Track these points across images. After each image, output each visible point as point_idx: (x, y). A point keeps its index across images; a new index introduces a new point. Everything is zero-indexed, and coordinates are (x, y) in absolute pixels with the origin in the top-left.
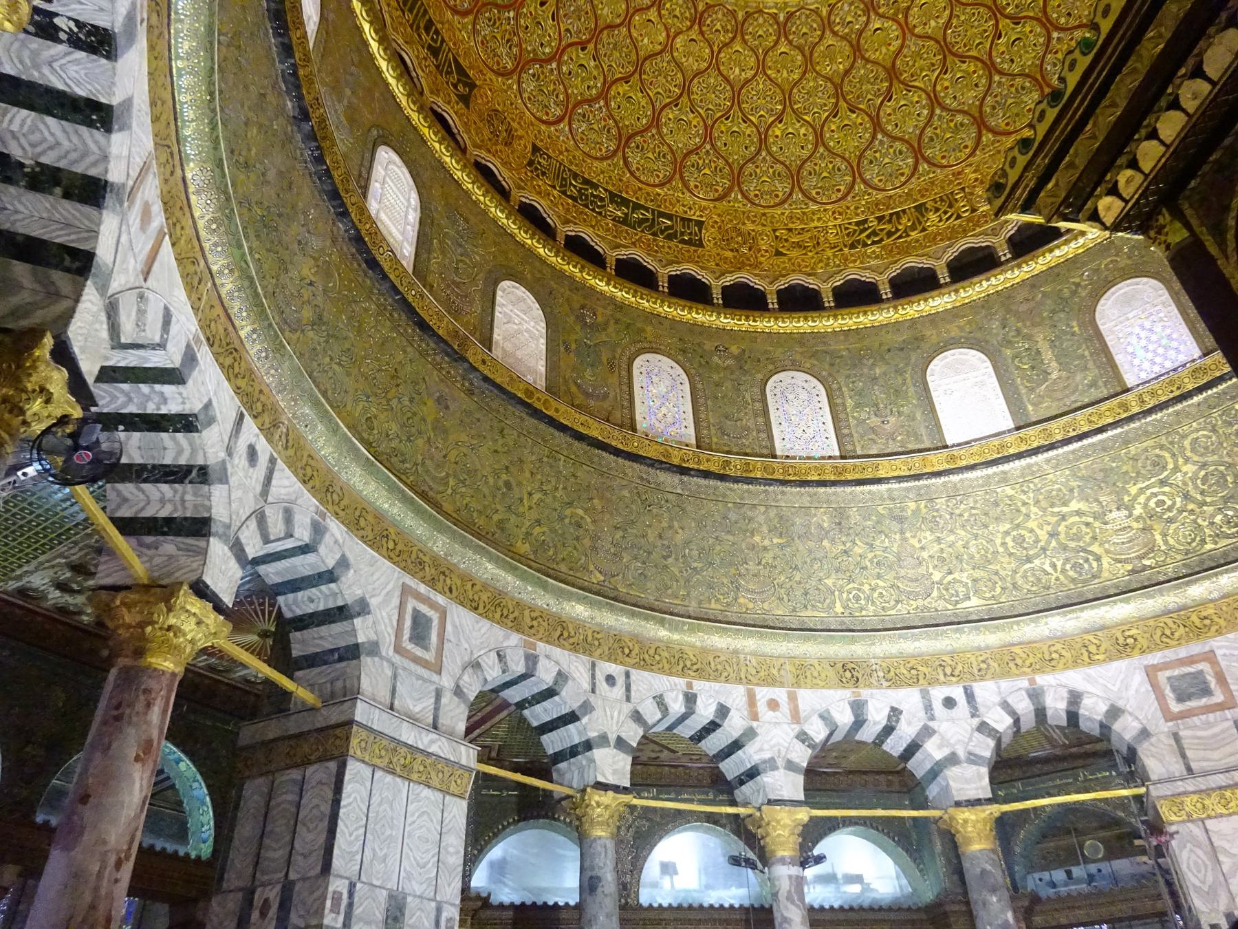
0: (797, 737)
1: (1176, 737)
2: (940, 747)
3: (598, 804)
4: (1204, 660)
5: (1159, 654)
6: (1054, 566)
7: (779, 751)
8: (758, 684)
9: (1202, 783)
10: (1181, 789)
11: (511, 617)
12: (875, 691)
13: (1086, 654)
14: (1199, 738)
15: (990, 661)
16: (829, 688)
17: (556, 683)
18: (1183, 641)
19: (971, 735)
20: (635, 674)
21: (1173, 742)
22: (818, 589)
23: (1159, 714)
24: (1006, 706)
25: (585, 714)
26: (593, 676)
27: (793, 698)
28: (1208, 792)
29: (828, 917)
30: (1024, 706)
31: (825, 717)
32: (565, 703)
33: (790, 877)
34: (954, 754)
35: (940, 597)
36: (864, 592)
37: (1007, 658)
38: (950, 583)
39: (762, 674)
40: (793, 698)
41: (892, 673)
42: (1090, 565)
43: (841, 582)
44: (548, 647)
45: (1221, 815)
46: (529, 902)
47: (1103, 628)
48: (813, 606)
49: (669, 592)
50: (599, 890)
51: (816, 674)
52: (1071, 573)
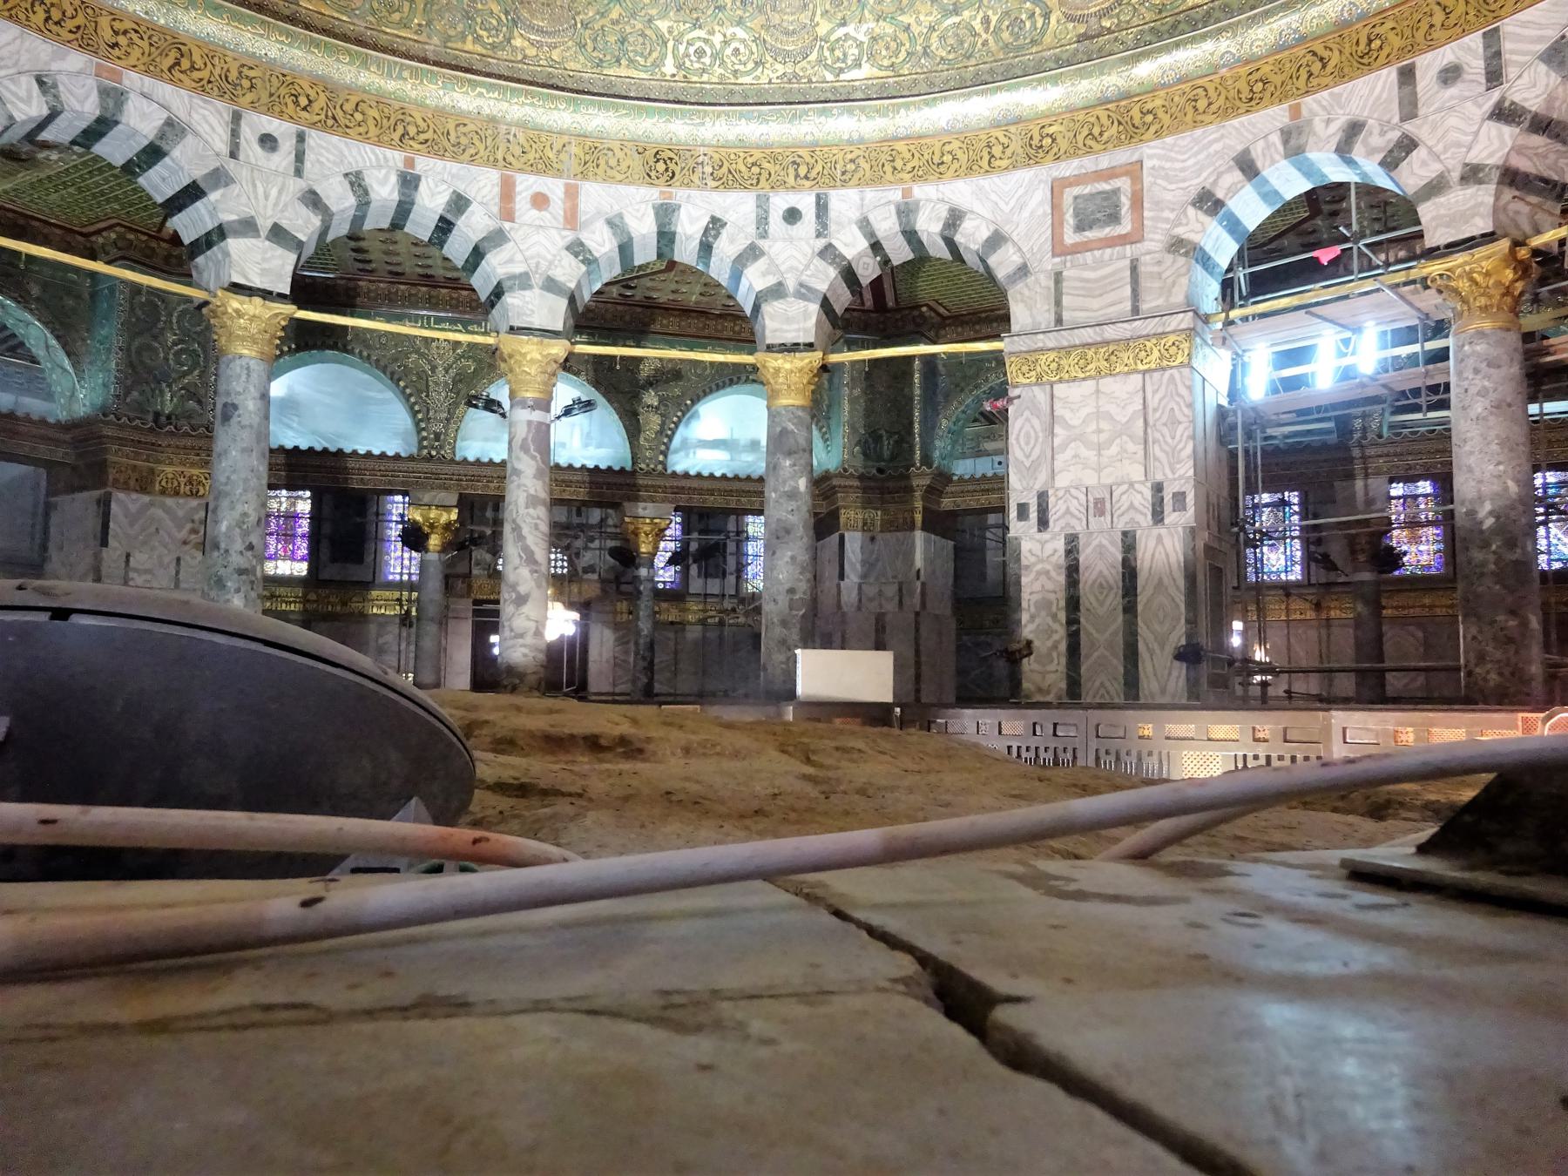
0: (568, 248)
1: (1058, 278)
2: (764, 274)
3: (239, 313)
4: (1126, 173)
5: (1075, 162)
6: (986, 21)
7: (538, 264)
8: (521, 170)
9: (1066, 338)
10: (1040, 345)
11: (70, 24)
12: (694, 193)
13: (986, 157)
14: (1087, 281)
15: (861, 161)
16: (630, 183)
17: (162, 135)
18: (1110, 145)
19: (810, 262)
20: (315, 138)
21: (1052, 284)
22: (643, 35)
23: (1048, 246)
24: (865, 225)
25: (216, 187)
26: (235, 134)
27: (572, 194)
28: (1067, 350)
29: (695, 484)
30: (887, 226)
31: (615, 224)
32: (182, 169)
33: (529, 423)
34: (780, 284)
35: (820, 61)
36: (712, 46)
37: (884, 158)
38: (837, 40)
39: (531, 156)
40: (572, 194)
41: (725, 169)
42: (1034, 24)
43: (682, 27)
44: (148, 80)
45: (1075, 379)
46: (318, 448)
47: (1018, 121)
48: (631, 61)
49: (396, 16)
50: (234, 420)
51: (613, 162)
52: (1006, 35)
